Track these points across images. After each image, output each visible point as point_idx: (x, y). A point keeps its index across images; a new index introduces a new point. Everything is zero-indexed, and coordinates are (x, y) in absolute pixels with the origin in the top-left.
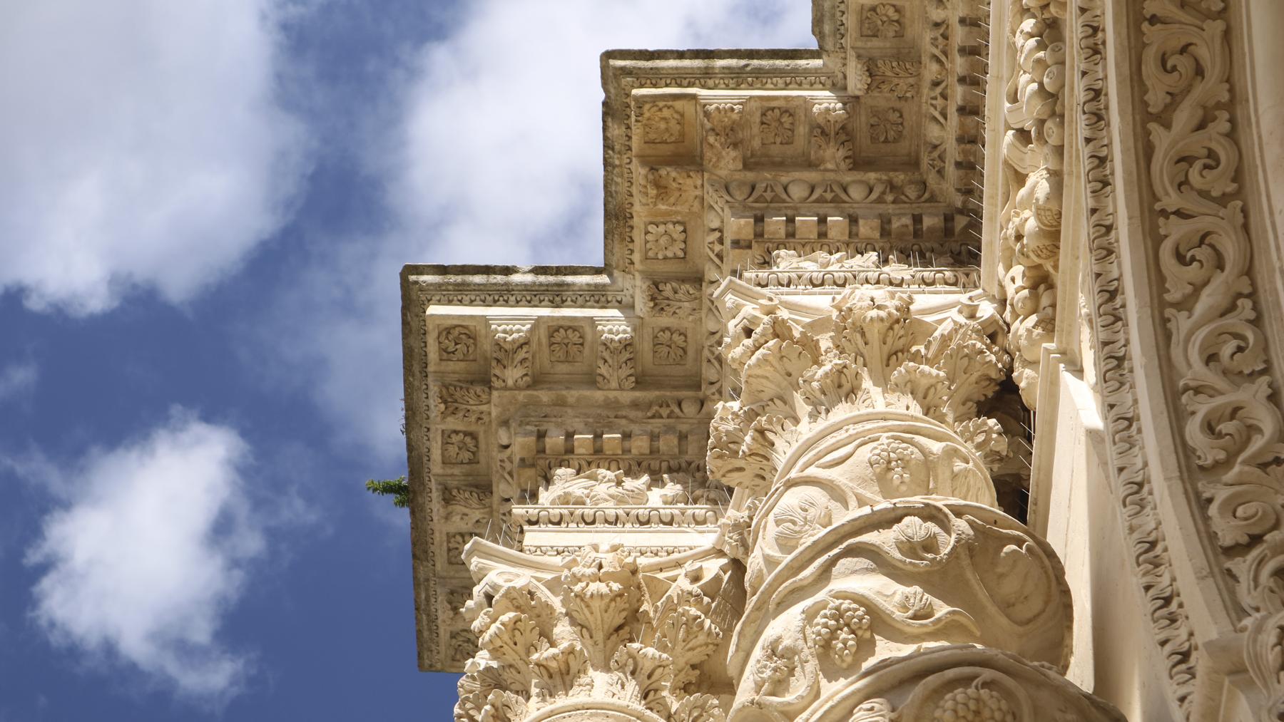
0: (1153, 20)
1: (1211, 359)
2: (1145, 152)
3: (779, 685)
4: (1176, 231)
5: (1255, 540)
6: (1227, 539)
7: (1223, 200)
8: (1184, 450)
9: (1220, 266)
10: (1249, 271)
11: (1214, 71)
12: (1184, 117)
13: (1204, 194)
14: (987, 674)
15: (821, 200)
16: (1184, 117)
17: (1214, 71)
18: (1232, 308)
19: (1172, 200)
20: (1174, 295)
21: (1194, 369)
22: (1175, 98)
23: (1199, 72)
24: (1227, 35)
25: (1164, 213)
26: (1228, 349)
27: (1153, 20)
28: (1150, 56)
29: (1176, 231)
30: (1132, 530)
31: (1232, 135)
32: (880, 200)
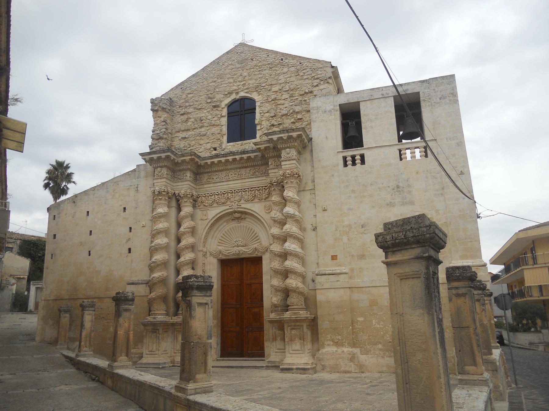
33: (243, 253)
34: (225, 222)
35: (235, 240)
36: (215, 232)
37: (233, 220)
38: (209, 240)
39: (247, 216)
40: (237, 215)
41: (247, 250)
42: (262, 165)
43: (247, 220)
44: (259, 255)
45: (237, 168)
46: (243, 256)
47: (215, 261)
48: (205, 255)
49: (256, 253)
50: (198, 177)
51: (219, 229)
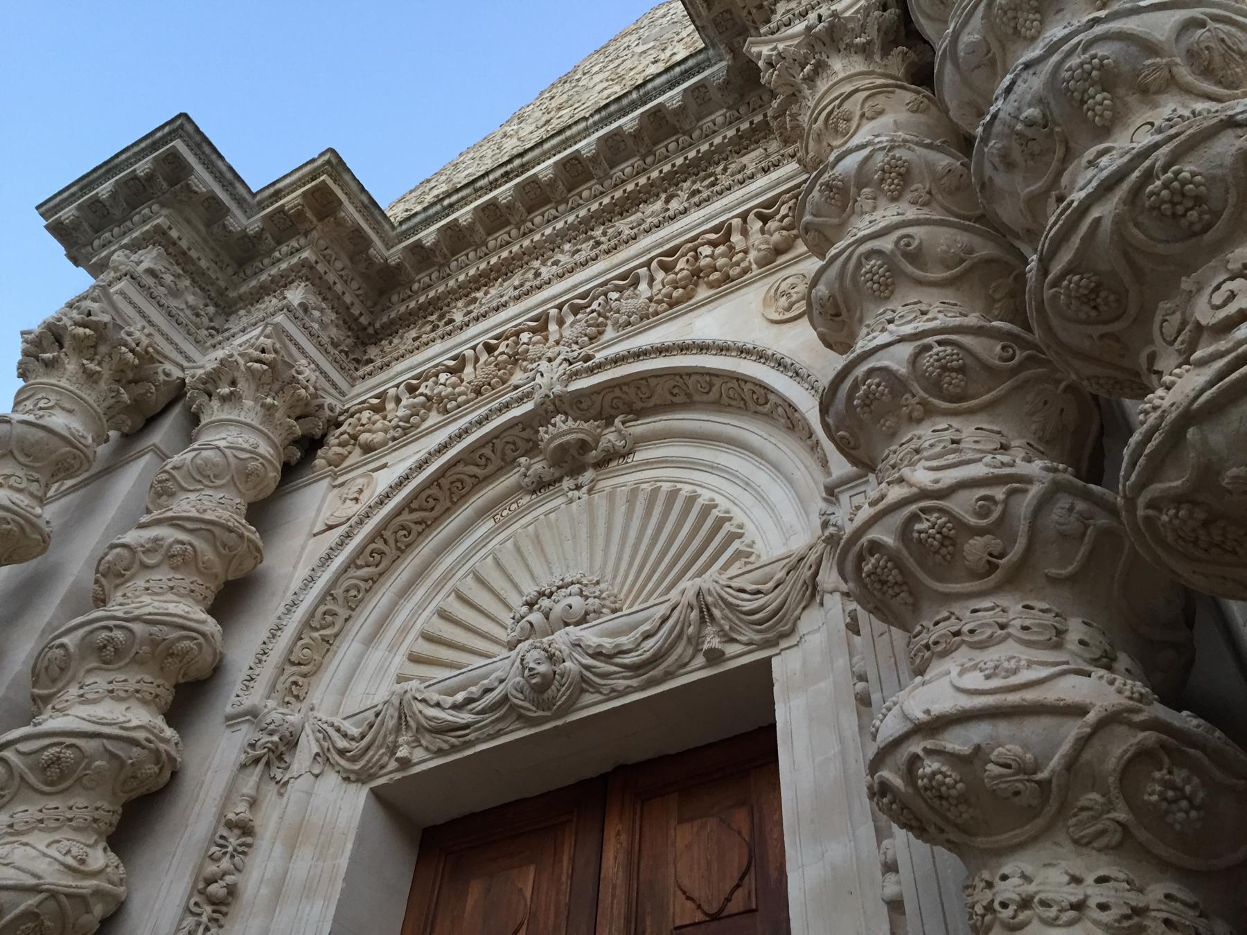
0: (439, 485)
1: (347, 591)
2: (398, 512)
3: (147, 551)
4: (379, 545)
5: (299, 664)
6: (293, 659)
7: (398, 549)
8: (312, 615)
9: (377, 566)
10: (381, 574)
11: (435, 513)
12: (416, 516)
13: (396, 541)
14: (201, 640)
15: (341, 276)
16: (416, 516)
17: (435, 513)
18: (366, 581)
19: (387, 534)
20: (359, 562)
21: (338, 592)
22: (421, 509)
23: (433, 509)
24: (448, 509)
25: (382, 536)
26: (353, 592)
27: (439, 485)
28: (428, 492)
29: (379, 545)
30: (279, 618)
31: (419, 534)
32: (358, 296)
33: (583, 684)
34: (482, 514)
35: (530, 590)
36: (405, 592)
37: (541, 486)
38: (348, 649)
39: (639, 427)
40: (563, 428)
41: (625, 641)
42: (742, 144)
43: (640, 456)
44: (739, 656)
45: (586, 225)
46: (593, 706)
47: (343, 806)
48: (274, 754)
49: (712, 641)
50: (373, 352)
51: (437, 573)
